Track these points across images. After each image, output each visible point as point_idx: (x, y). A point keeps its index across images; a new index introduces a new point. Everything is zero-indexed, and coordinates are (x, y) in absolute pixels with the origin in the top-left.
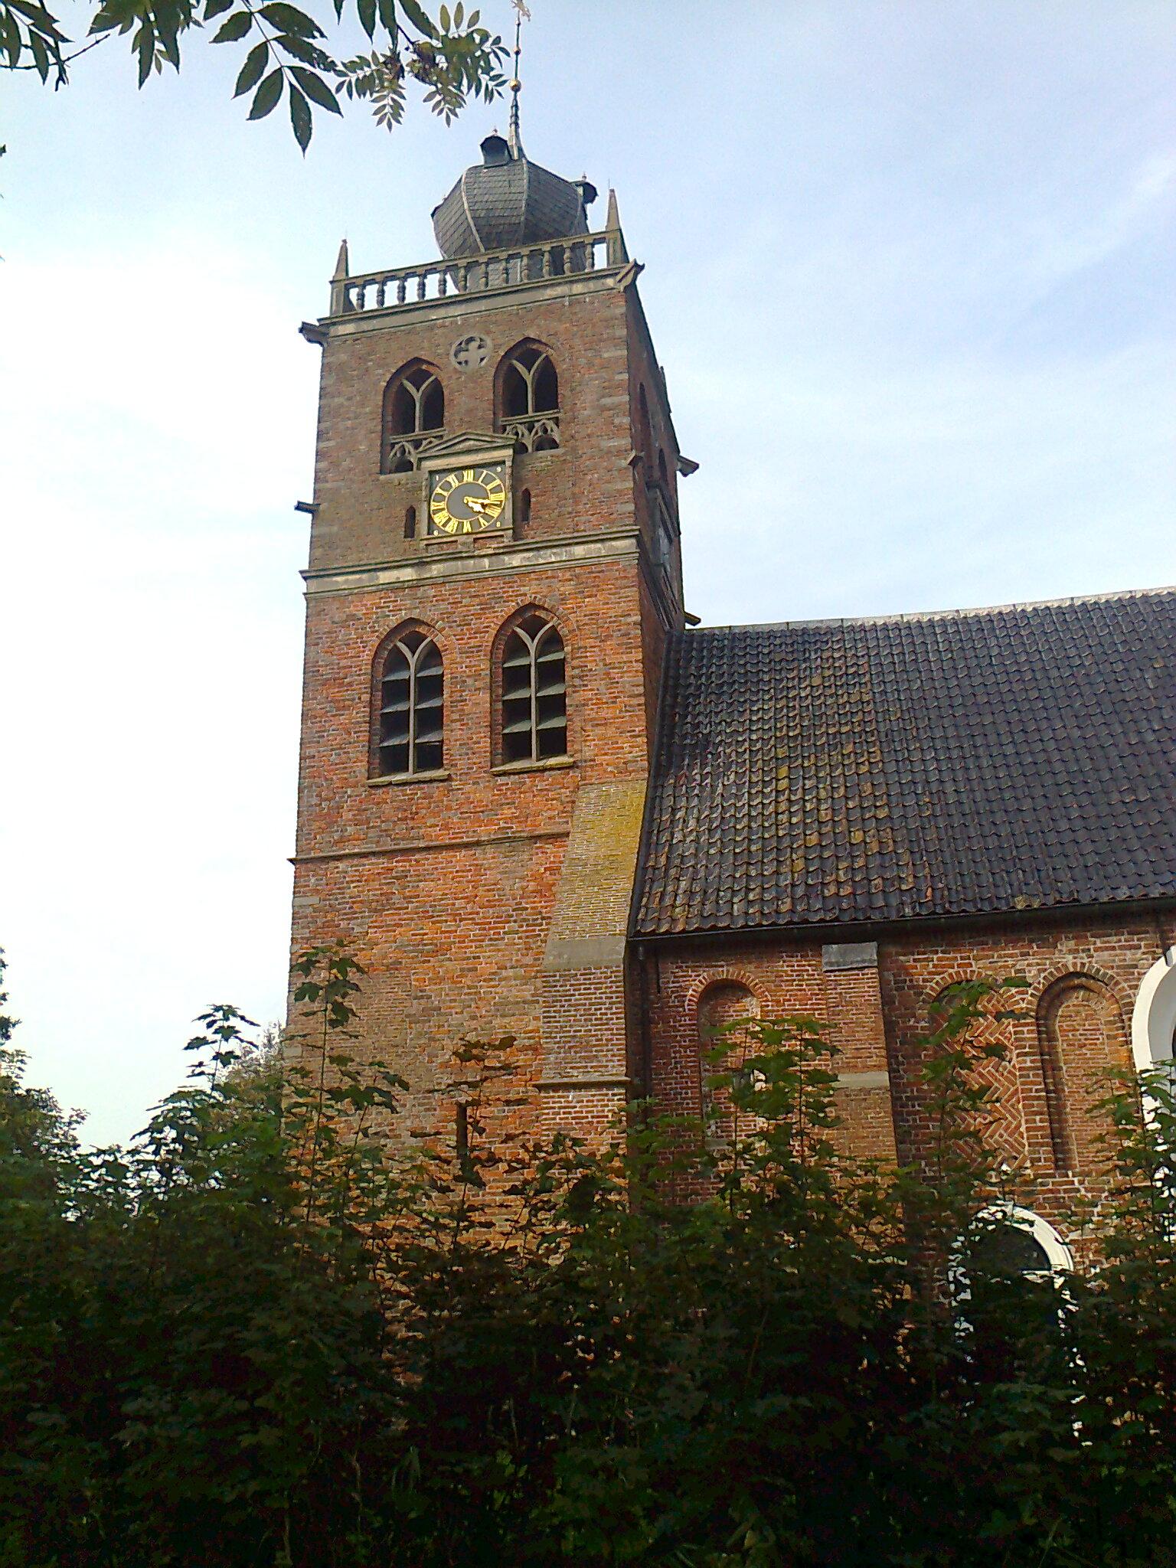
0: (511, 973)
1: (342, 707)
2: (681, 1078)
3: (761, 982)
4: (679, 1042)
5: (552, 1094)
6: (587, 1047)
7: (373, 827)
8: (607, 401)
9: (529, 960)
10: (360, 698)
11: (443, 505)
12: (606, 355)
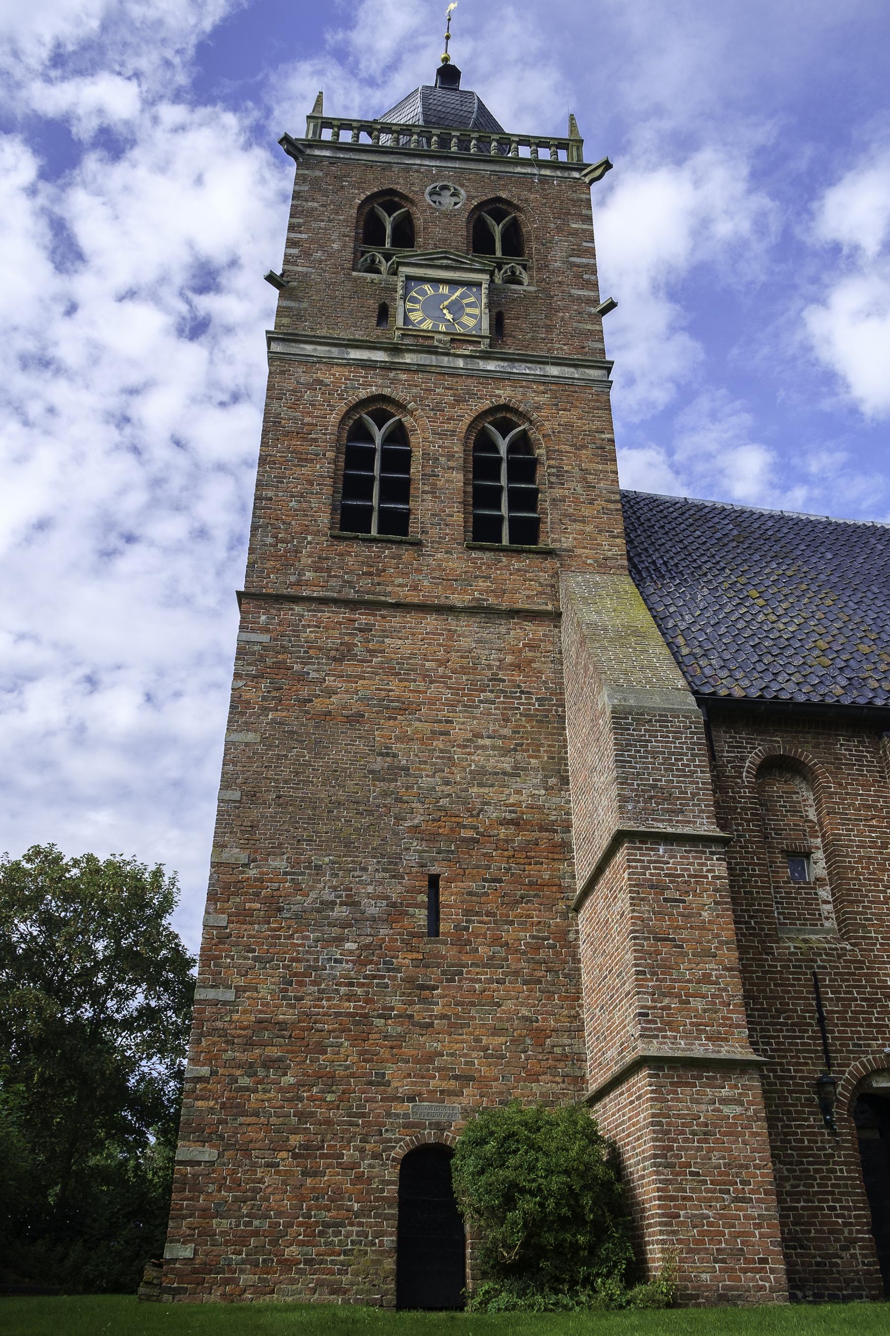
0: (487, 742)
1: (303, 460)
2: (746, 852)
3: (820, 762)
4: (739, 814)
5: (638, 845)
6: (669, 798)
7: (335, 576)
9: (506, 732)
10: (324, 455)
11: (417, 306)
12: (574, 226)
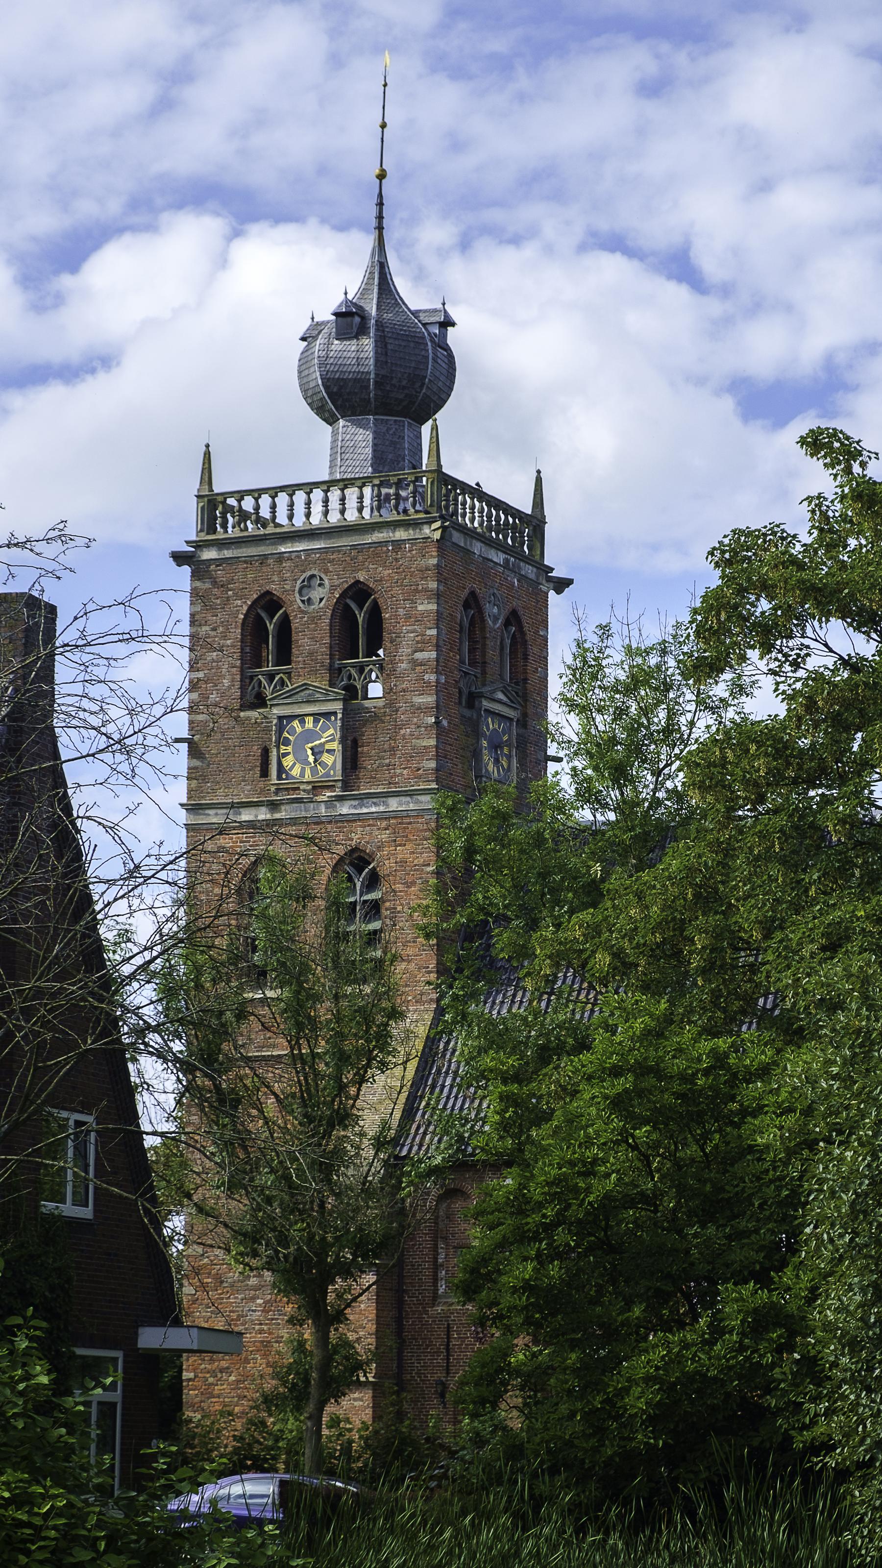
8: (419, 656)
11: (290, 749)
